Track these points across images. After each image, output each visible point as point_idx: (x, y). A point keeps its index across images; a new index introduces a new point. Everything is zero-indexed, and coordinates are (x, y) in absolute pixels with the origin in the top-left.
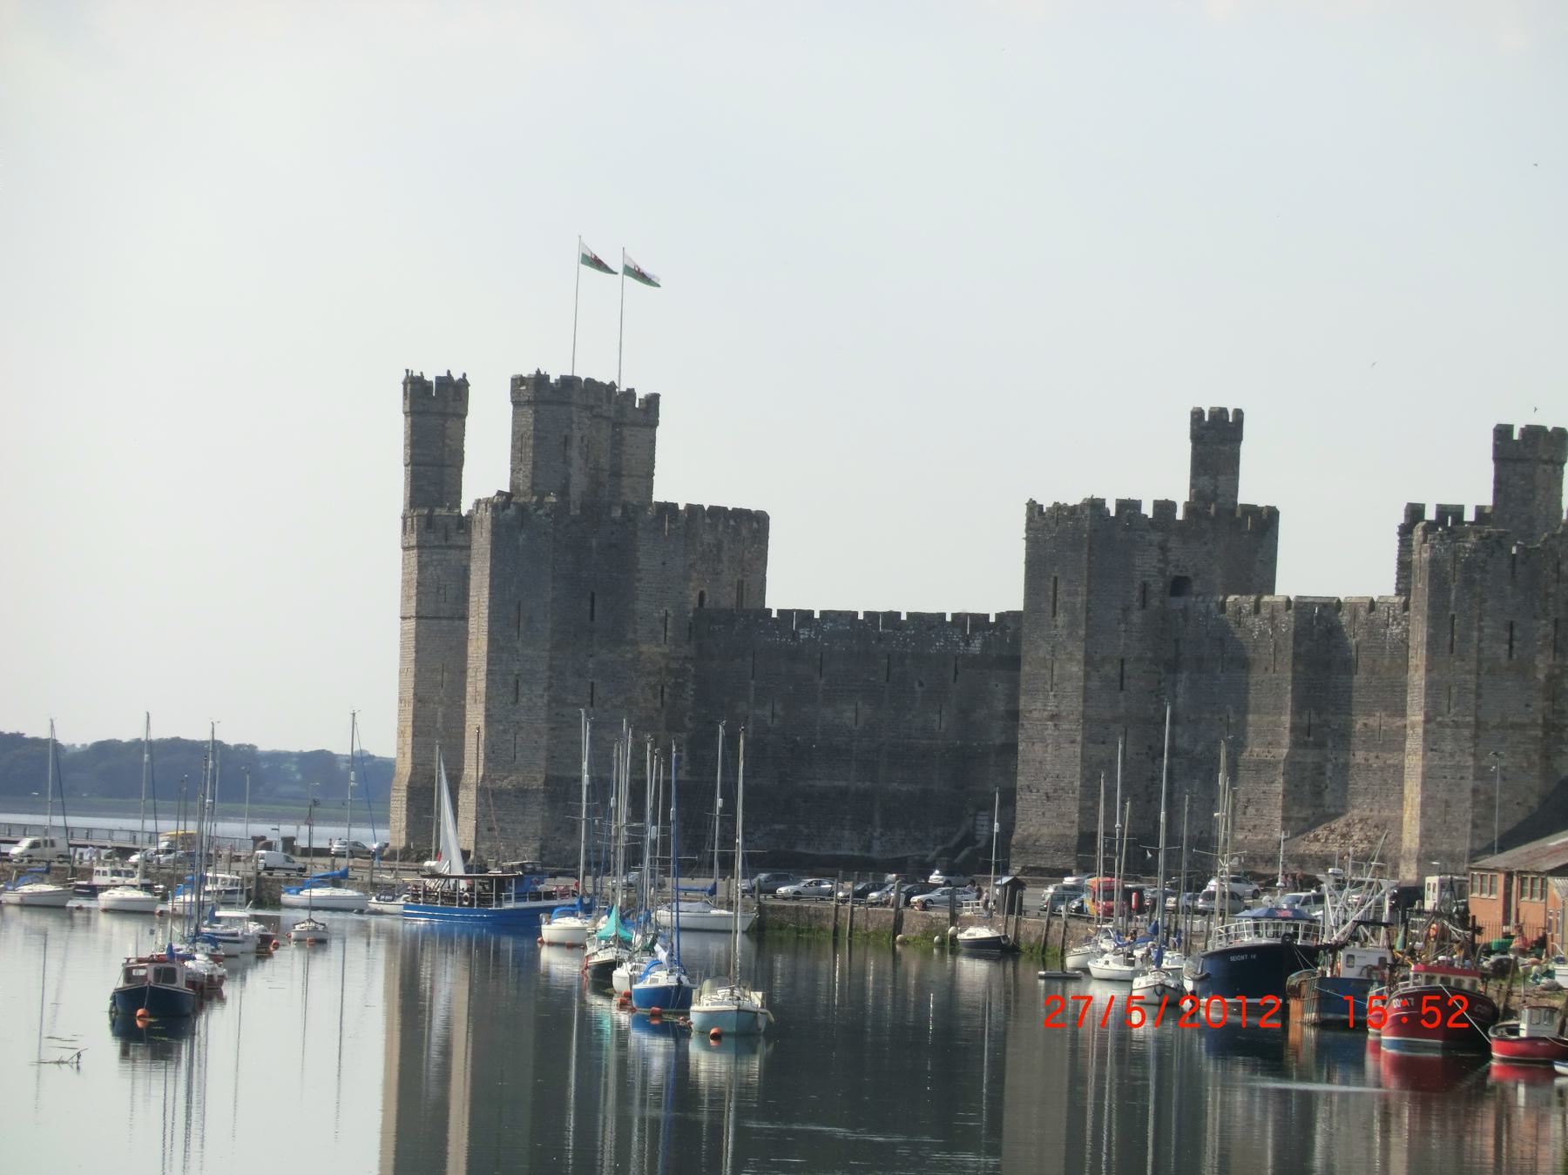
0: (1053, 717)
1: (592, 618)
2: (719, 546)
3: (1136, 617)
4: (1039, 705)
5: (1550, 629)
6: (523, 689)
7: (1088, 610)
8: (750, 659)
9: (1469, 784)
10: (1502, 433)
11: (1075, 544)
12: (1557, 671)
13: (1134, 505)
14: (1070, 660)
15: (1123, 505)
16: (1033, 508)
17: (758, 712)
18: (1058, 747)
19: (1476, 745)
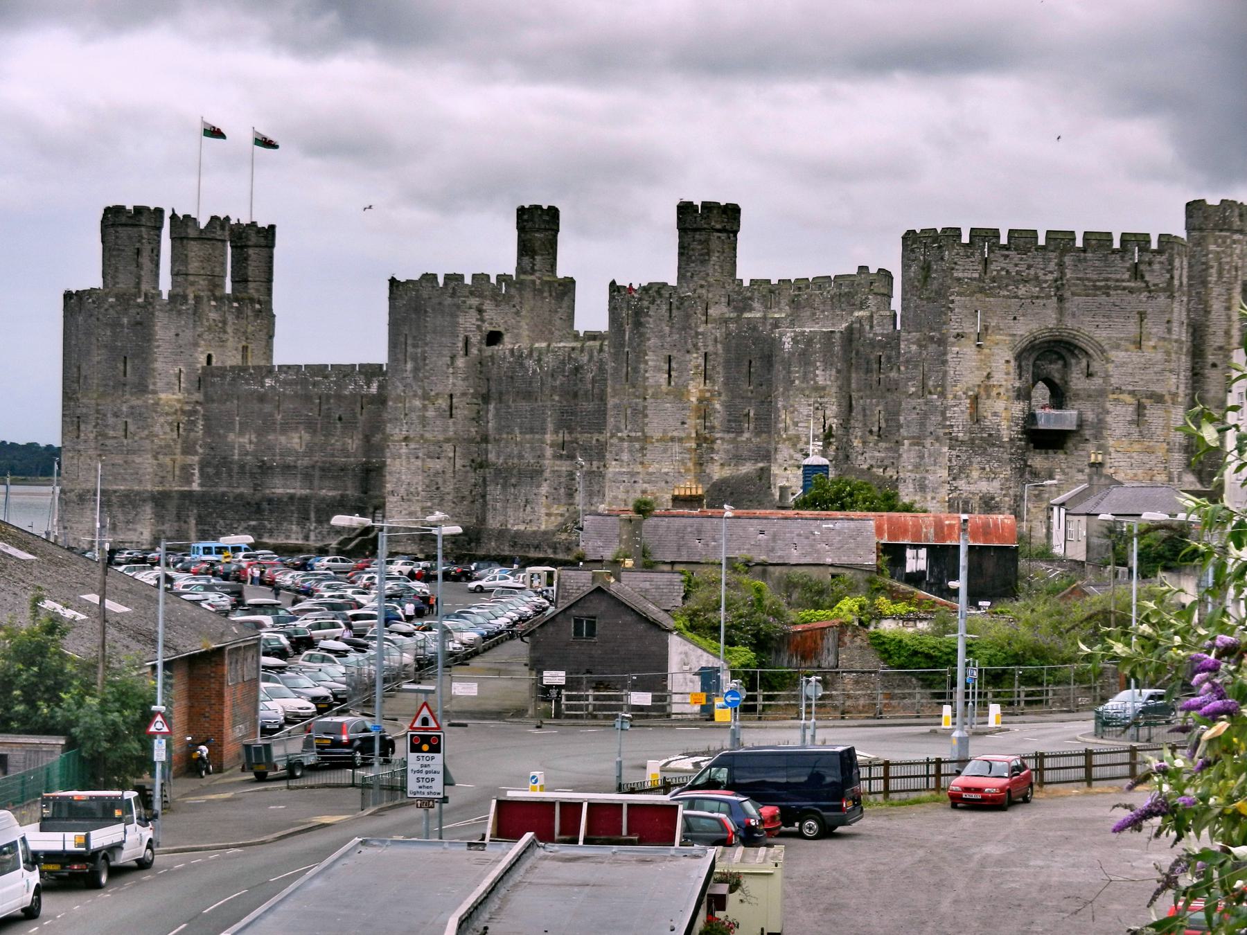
0: (406, 439)
2: (224, 322)
5: (701, 361)
6: (82, 427)
12: (708, 395)
14: (415, 396)
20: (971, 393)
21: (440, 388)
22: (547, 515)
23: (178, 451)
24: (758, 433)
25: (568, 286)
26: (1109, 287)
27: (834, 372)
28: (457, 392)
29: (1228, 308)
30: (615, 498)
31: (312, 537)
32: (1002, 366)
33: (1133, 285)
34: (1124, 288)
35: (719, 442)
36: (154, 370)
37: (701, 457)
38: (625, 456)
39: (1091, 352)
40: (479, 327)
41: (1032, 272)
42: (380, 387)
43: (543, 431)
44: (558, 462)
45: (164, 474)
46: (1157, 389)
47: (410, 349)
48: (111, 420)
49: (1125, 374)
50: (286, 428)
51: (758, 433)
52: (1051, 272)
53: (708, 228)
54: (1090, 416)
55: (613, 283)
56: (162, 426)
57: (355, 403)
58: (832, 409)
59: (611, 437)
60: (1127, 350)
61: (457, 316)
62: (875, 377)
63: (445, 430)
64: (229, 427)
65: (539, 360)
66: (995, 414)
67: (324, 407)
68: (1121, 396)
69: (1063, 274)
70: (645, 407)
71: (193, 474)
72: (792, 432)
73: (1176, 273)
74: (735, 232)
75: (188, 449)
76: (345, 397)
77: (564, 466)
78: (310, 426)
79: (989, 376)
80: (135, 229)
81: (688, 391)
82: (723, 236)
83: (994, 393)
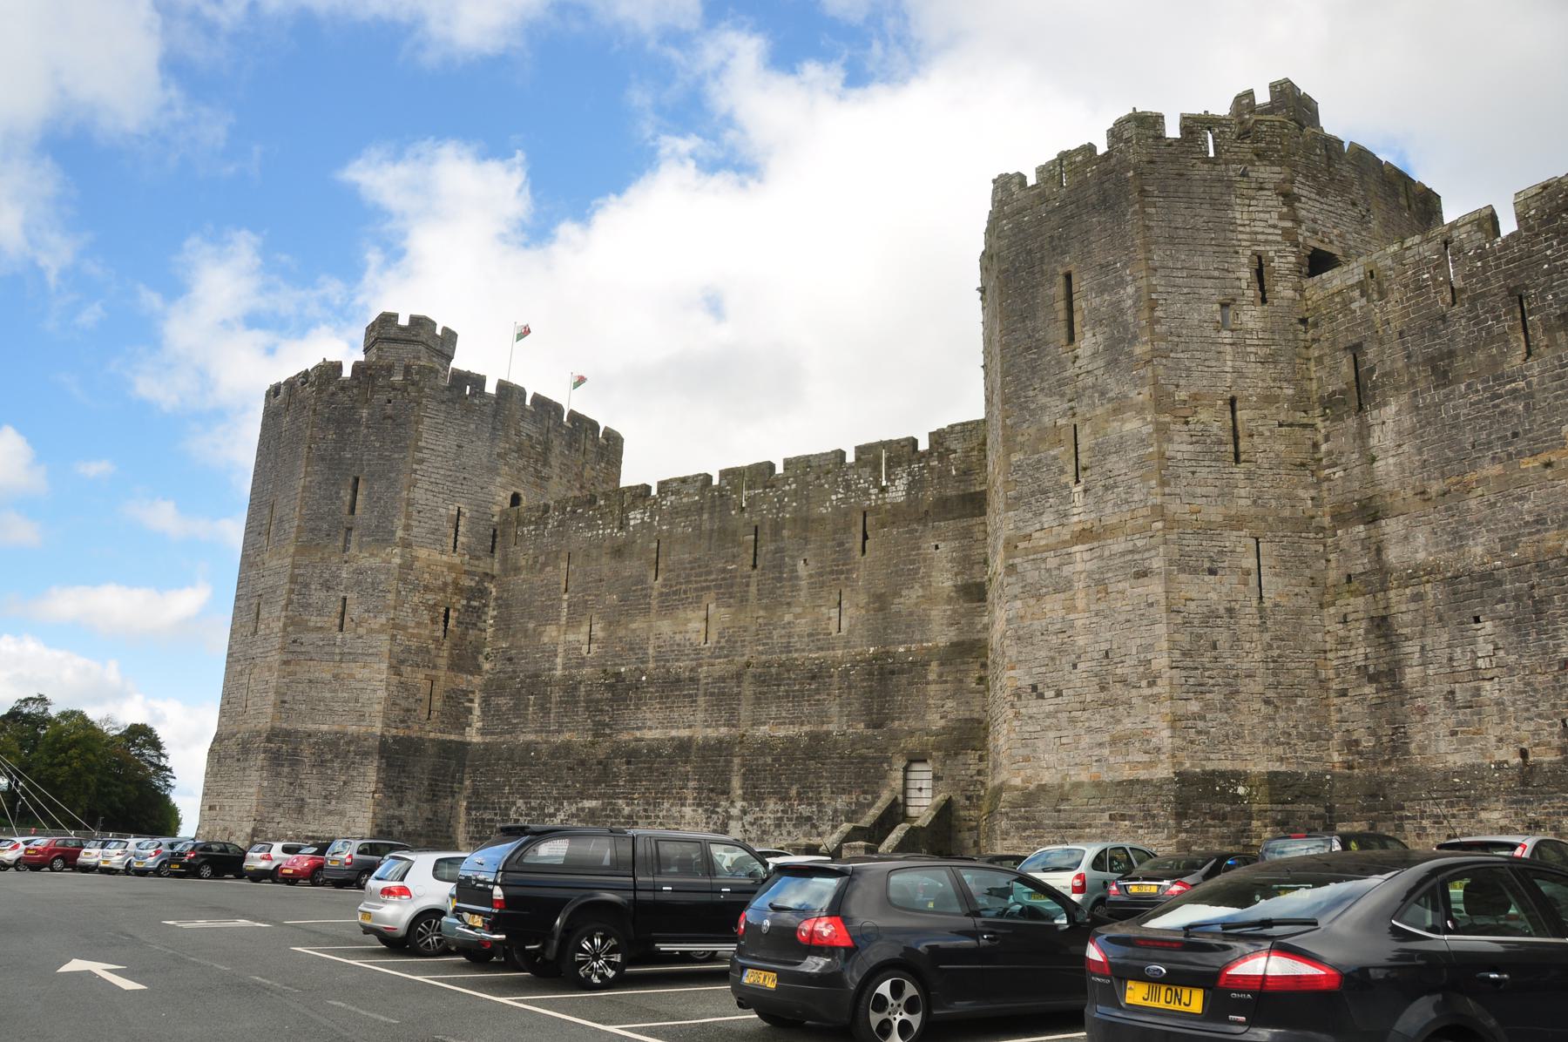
1: (352, 511)
2: (547, 449)
3: (1251, 317)
4: (1048, 519)
8: (564, 565)
17: (571, 637)
21: (1200, 383)
23: (443, 662)
28: (1251, 390)
36: (410, 503)
45: (410, 703)
48: (317, 596)
50: (670, 603)
56: (415, 611)
57: (847, 529)
61: (1229, 206)
63: (1226, 493)
64: (547, 615)
67: (767, 548)
71: (470, 711)
75: (464, 661)
76: (822, 519)
78: (729, 590)
80: (410, 347)
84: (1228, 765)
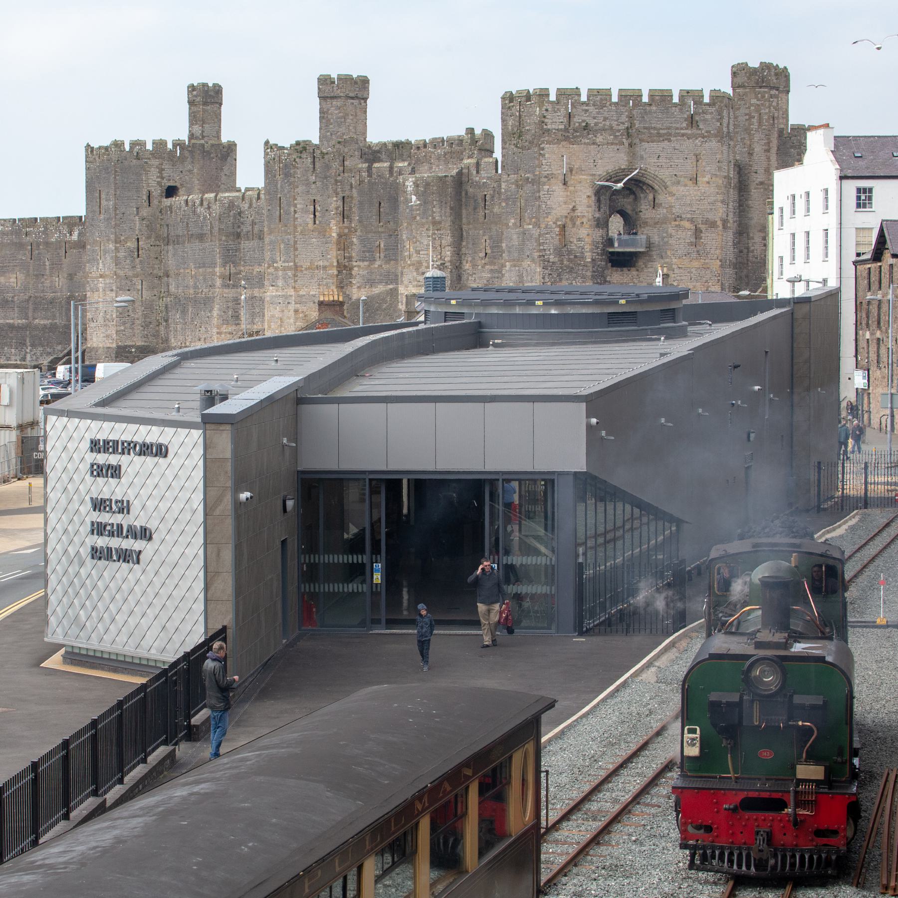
5: (340, 203)
7: (116, 209)
9: (292, 307)
10: (324, 81)
11: (113, 168)
12: (346, 231)
13: (142, 144)
14: (108, 240)
15: (133, 144)
16: (89, 149)
18: (105, 295)
19: (296, 281)
20: (559, 223)
22: (218, 333)
24: (388, 259)
25: (231, 148)
26: (670, 135)
27: (448, 210)
29: (768, 151)
30: (273, 316)
31: (28, 357)
32: (585, 201)
33: (690, 132)
34: (683, 135)
35: (356, 269)
37: (341, 283)
38: (280, 283)
39: (656, 187)
40: (159, 183)
41: (608, 123)
42: (79, 234)
43: (213, 265)
44: (226, 291)
46: (711, 216)
47: (104, 203)
49: (684, 205)
51: (388, 259)
52: (623, 123)
53: (344, 96)
54: (656, 239)
55: (267, 143)
57: (60, 248)
58: (448, 239)
59: (268, 268)
60: (686, 185)
62: (481, 213)
65: (209, 208)
66: (579, 240)
68: (682, 223)
69: (632, 125)
70: (295, 242)
72: (415, 258)
73: (725, 121)
74: (365, 99)
76: (52, 243)
77: (230, 293)
79: (574, 209)
81: (331, 229)
82: (356, 102)
83: (578, 223)
84: (131, 343)
